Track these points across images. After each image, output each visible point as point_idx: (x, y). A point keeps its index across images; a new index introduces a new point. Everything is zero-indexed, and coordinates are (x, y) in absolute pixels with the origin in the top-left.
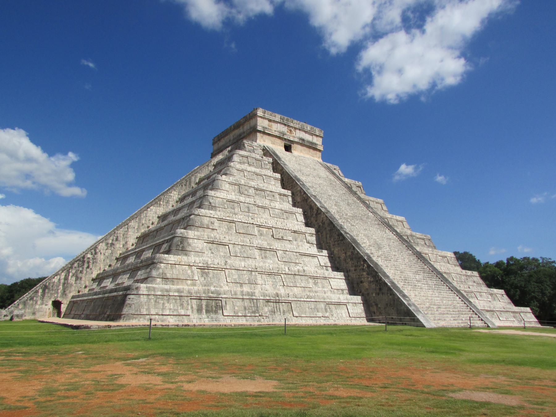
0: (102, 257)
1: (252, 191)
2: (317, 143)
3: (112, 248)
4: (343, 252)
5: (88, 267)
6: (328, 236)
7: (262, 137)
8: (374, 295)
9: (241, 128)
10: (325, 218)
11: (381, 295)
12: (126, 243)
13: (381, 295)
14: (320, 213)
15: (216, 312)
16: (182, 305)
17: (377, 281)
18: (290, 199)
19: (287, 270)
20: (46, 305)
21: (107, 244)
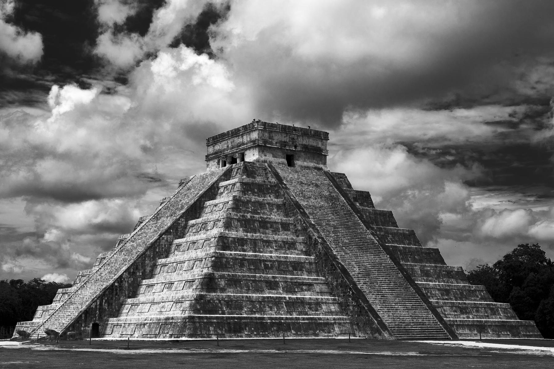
2: (323, 147)
5: (116, 294)
12: (145, 271)
14: (317, 244)
15: (240, 332)
19: (288, 299)
21: (129, 273)
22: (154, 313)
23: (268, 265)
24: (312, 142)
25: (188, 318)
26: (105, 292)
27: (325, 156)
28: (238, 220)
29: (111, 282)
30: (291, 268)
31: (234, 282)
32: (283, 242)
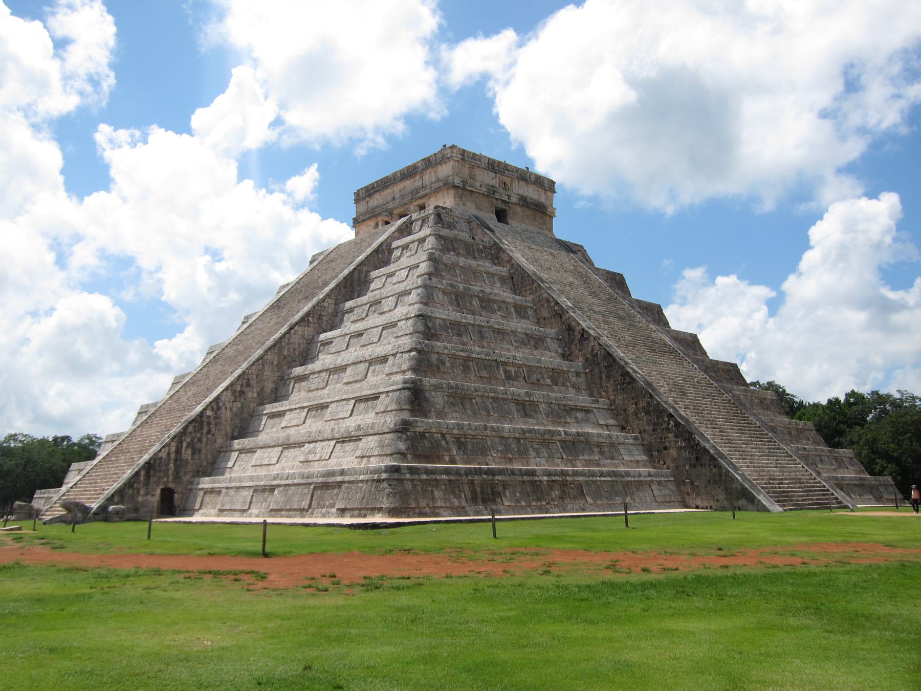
0: (228, 414)
1: (476, 302)
2: (547, 203)
3: (242, 400)
4: (632, 401)
5: (209, 432)
6: (604, 376)
7: (461, 197)
8: (687, 468)
9: (417, 177)
10: (597, 347)
11: (699, 467)
12: (262, 389)
13: (699, 467)
14: (586, 339)
15: (494, 502)
16: (453, 492)
17: (692, 447)
18: (530, 313)
20: (153, 495)
21: (234, 392)
22: (290, 464)
23: (510, 372)
24: (532, 193)
25: (386, 472)
26: (185, 428)
27: (551, 217)
28: (444, 292)
29: (199, 409)
30: (549, 381)
31: (459, 399)
32: (526, 334)
